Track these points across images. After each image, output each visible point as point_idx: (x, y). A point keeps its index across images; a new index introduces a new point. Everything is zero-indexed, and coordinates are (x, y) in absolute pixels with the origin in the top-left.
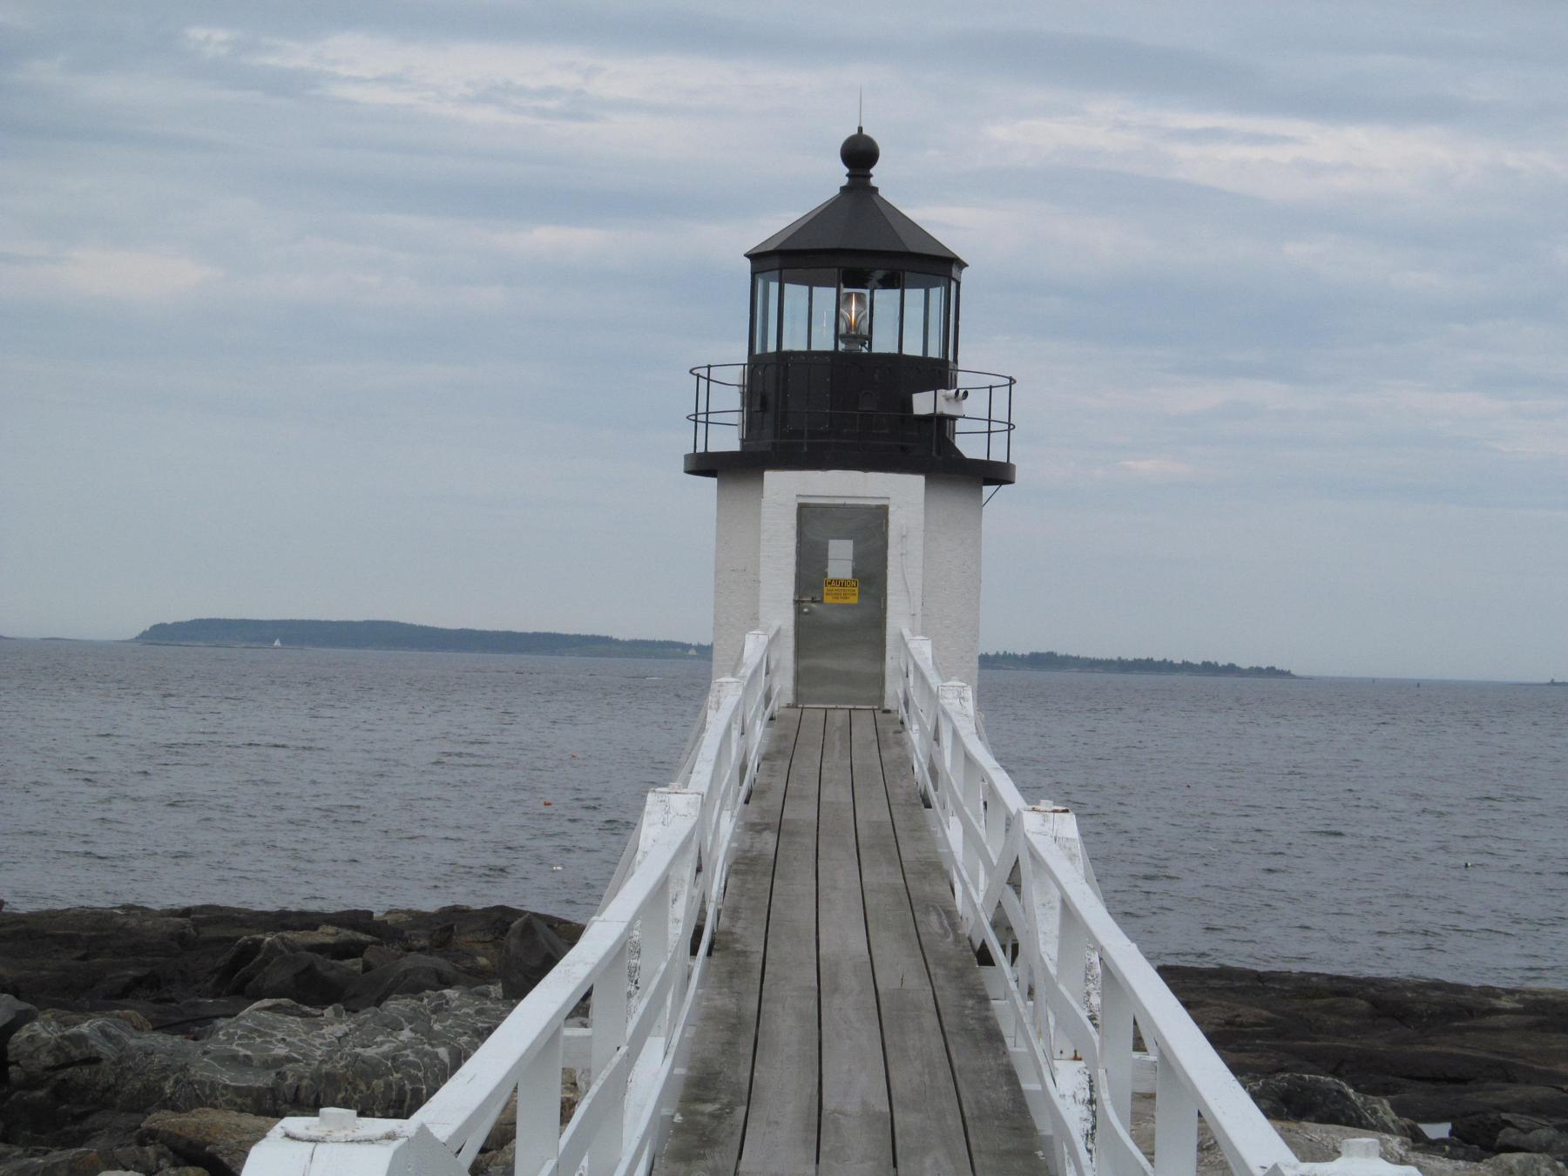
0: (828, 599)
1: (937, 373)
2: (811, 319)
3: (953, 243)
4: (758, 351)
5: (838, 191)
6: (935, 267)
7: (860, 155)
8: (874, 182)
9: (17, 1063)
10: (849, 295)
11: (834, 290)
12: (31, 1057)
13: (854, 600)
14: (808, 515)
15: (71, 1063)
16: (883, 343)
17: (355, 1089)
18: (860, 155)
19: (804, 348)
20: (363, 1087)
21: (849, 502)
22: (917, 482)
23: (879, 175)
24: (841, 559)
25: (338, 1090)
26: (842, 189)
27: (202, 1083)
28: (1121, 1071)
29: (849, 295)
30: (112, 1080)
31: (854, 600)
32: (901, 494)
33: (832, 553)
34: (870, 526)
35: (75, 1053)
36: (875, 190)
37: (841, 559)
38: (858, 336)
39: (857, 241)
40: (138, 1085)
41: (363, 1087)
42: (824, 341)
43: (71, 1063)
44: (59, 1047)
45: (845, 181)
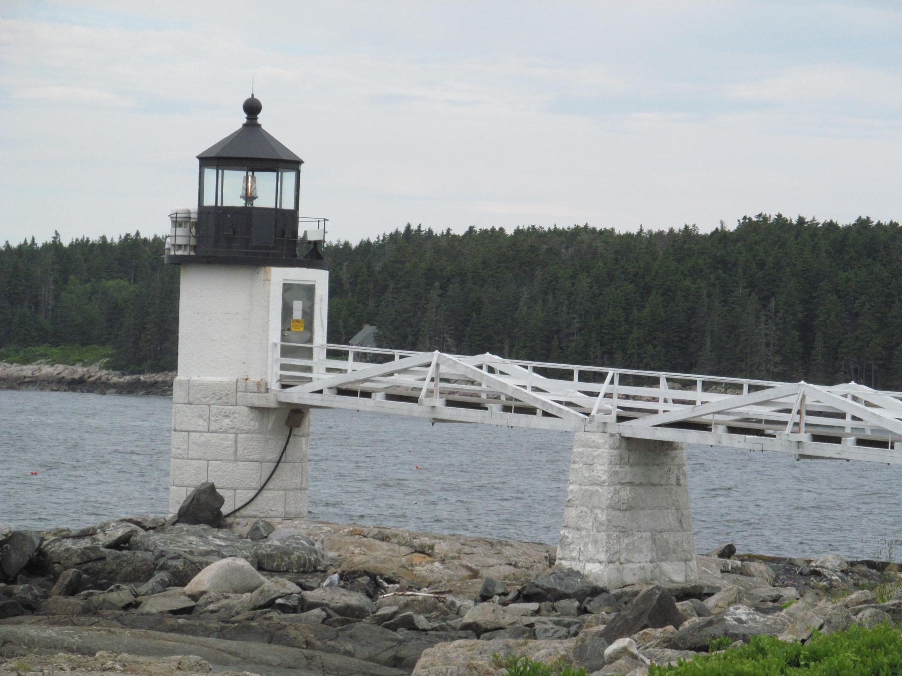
0: (293, 329)
2: (232, 189)
3: (299, 153)
4: (219, 204)
5: (241, 126)
6: (294, 164)
7: (252, 108)
8: (259, 121)
9: (59, 563)
11: (215, 171)
12: (67, 559)
13: (302, 330)
14: (287, 288)
15: (91, 560)
16: (265, 200)
17: (282, 560)
18: (252, 108)
19: (272, 206)
20: (286, 559)
21: (301, 283)
23: (261, 119)
25: (274, 561)
26: (244, 125)
30: (114, 567)
33: (295, 308)
35: (92, 555)
36: (259, 126)
38: (249, 198)
39: (251, 150)
40: (130, 569)
41: (286, 559)
42: (233, 199)
43: (91, 560)
44: (83, 553)
45: (244, 121)
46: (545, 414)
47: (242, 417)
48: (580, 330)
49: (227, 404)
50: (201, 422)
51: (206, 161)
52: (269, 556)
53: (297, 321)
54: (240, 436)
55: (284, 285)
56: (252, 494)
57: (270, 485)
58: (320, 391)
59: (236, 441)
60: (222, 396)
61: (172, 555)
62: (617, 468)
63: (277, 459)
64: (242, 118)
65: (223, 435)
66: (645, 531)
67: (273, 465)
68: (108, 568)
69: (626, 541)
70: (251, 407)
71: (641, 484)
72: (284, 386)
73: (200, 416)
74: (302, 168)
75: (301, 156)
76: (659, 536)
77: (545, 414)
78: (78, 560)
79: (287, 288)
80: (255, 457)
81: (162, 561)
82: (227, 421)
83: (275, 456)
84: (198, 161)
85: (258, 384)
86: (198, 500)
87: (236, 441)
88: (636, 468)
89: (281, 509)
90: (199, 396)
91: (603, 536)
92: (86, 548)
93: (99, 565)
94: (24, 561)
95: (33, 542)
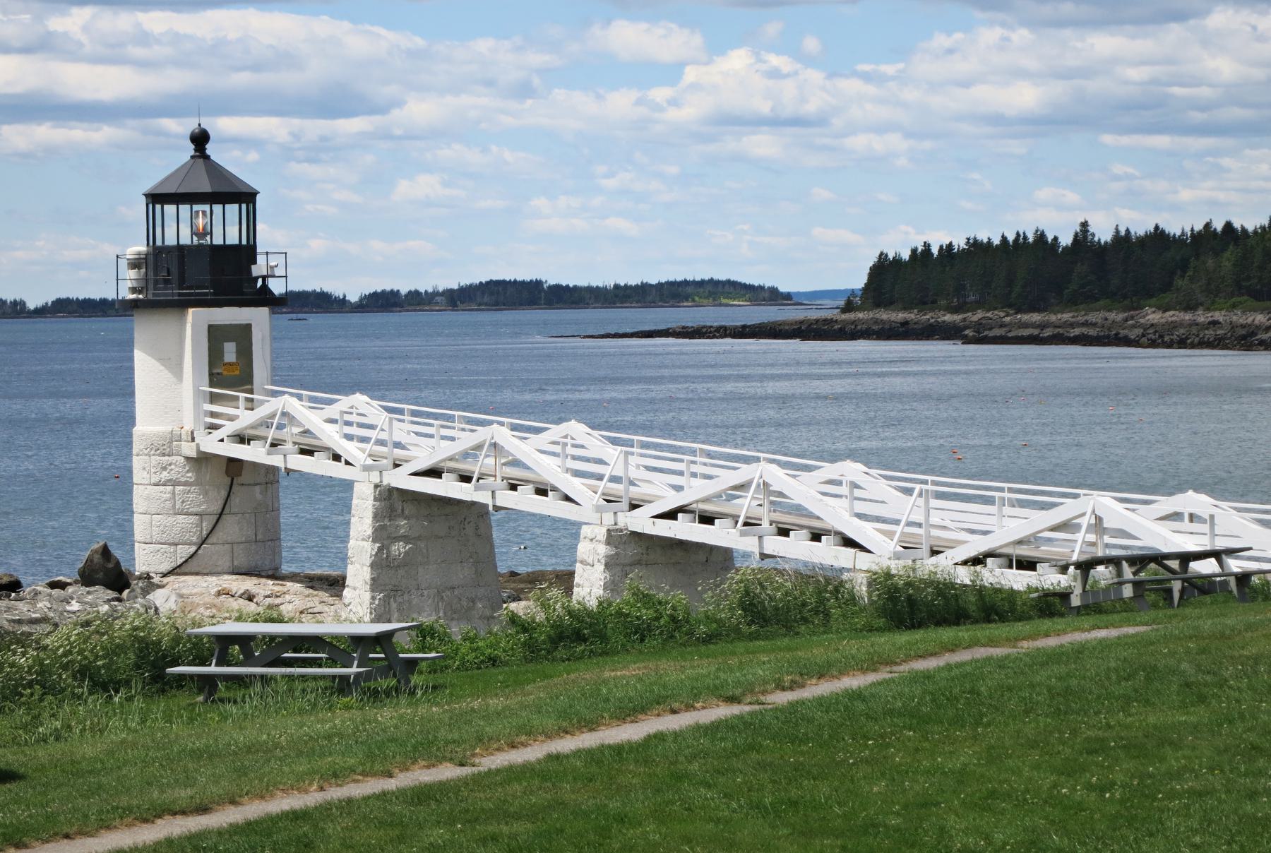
1: (247, 252)
2: (179, 227)
4: (159, 243)
6: (246, 197)
7: (200, 139)
8: (208, 152)
10: (197, 212)
14: (211, 328)
18: (200, 139)
22: (264, 311)
23: (210, 149)
24: (230, 352)
28: (286, 609)
29: (197, 212)
31: (237, 372)
32: (257, 317)
33: (226, 349)
34: (243, 334)
37: (230, 352)
46: (347, 463)
47: (178, 468)
49: (164, 455)
51: (156, 198)
53: (230, 364)
54: (179, 488)
55: (210, 327)
56: (193, 548)
57: (213, 539)
58: (222, 440)
59: (174, 494)
60: (166, 446)
62: (387, 522)
64: (190, 149)
65: (162, 488)
66: (428, 588)
67: (216, 517)
69: (399, 599)
71: (419, 538)
75: (258, 189)
76: (448, 593)
77: (347, 463)
79: (211, 328)
82: (165, 473)
83: (216, 507)
84: (144, 199)
87: (174, 494)
88: (413, 521)
89: (228, 564)
91: (368, 595)
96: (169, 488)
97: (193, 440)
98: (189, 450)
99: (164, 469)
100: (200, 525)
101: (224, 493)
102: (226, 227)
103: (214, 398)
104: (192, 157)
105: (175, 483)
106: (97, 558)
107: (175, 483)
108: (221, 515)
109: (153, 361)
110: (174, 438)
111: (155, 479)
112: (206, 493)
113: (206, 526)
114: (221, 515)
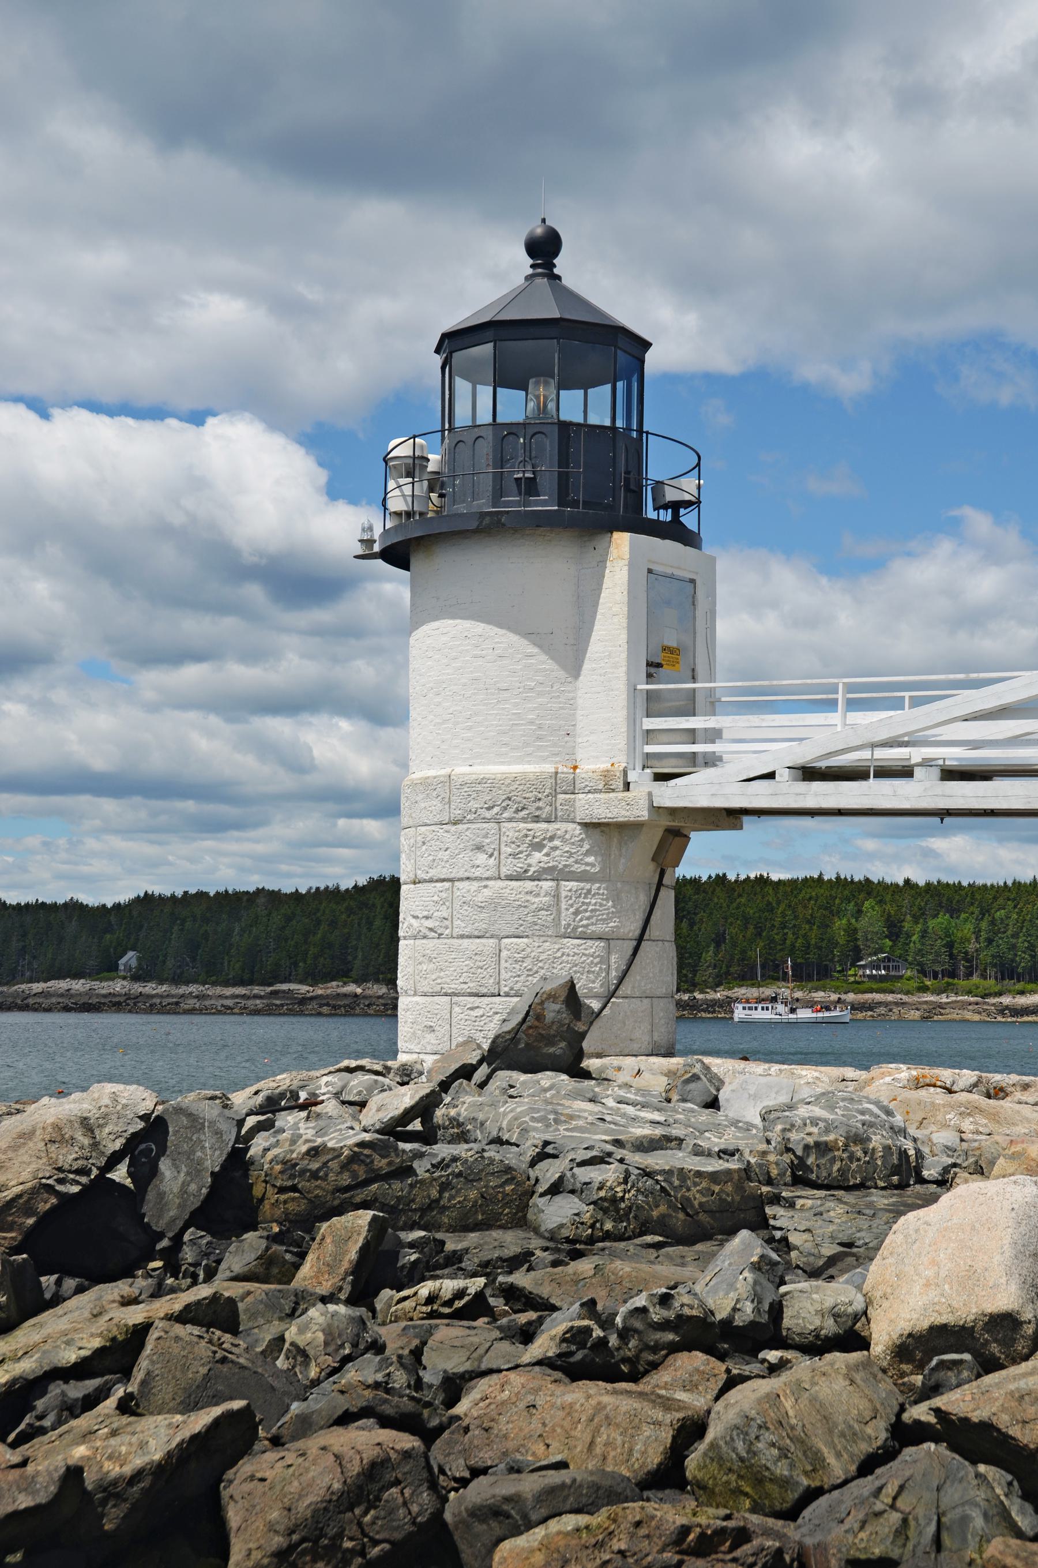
27: (669, 1173)
35: (381, 1163)
44: (354, 1158)
47: (568, 844)
48: (274, 949)
49: (537, 819)
50: (481, 858)
52: (822, 1148)
54: (568, 886)
57: (625, 989)
58: (771, 776)
59: (557, 896)
61: (582, 1155)
63: (638, 932)
64: (524, 263)
65: (529, 885)
68: (420, 1199)
70: (586, 825)
72: (662, 777)
73: (479, 848)
74: (649, 356)
78: (346, 1180)
80: (599, 928)
81: (549, 1172)
82: (537, 856)
83: (634, 928)
85: (606, 775)
86: (539, 1017)
89: (646, 1038)
90: (474, 805)
92: (362, 1144)
93: (398, 1187)
94: (200, 1189)
95: (218, 1133)
96: (547, 885)
97: (627, 786)
98: (631, 806)
99: (538, 846)
100: (605, 960)
101: (643, 900)
102: (590, 406)
103: (654, 705)
104: (528, 278)
105: (558, 875)
106: (553, 1011)
107: (558, 875)
108: (640, 939)
109: (513, 638)
110: (564, 785)
111: (519, 866)
112: (616, 898)
113: (617, 961)
114: (640, 939)
